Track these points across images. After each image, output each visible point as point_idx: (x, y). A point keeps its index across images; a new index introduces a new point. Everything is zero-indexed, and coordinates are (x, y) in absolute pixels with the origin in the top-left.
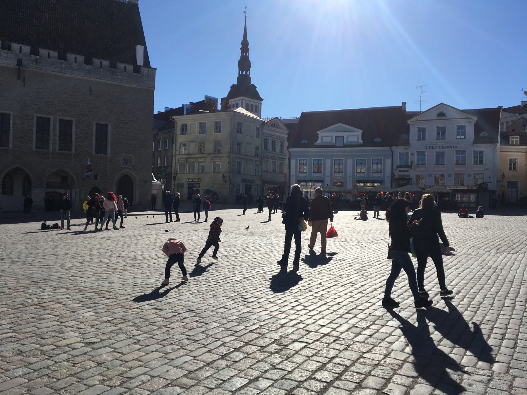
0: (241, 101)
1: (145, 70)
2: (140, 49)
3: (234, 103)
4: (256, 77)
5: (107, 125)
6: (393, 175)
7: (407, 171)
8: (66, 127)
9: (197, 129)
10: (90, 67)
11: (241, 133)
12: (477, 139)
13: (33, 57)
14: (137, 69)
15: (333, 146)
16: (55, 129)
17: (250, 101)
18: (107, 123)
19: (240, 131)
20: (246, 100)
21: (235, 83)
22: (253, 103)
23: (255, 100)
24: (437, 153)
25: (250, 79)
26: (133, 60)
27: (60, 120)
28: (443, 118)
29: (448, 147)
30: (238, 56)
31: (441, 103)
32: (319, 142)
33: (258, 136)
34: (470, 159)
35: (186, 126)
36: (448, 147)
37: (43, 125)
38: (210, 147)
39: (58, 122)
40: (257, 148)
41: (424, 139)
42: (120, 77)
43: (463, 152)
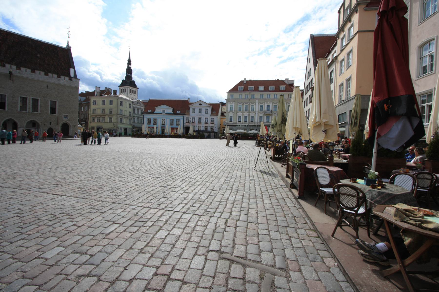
1: (74, 80)
2: (72, 70)
4: (135, 77)
5: (56, 102)
6: (184, 125)
8: (35, 102)
9: (101, 103)
10: (47, 77)
12: (212, 114)
13: (18, 71)
14: (70, 78)
16: (29, 102)
19: (121, 105)
21: (125, 79)
25: (132, 78)
26: (68, 75)
27: (32, 99)
30: (126, 66)
32: (156, 112)
33: (130, 107)
34: (209, 121)
35: (95, 101)
37: (24, 100)
38: (107, 112)
39: (31, 100)
40: (130, 112)
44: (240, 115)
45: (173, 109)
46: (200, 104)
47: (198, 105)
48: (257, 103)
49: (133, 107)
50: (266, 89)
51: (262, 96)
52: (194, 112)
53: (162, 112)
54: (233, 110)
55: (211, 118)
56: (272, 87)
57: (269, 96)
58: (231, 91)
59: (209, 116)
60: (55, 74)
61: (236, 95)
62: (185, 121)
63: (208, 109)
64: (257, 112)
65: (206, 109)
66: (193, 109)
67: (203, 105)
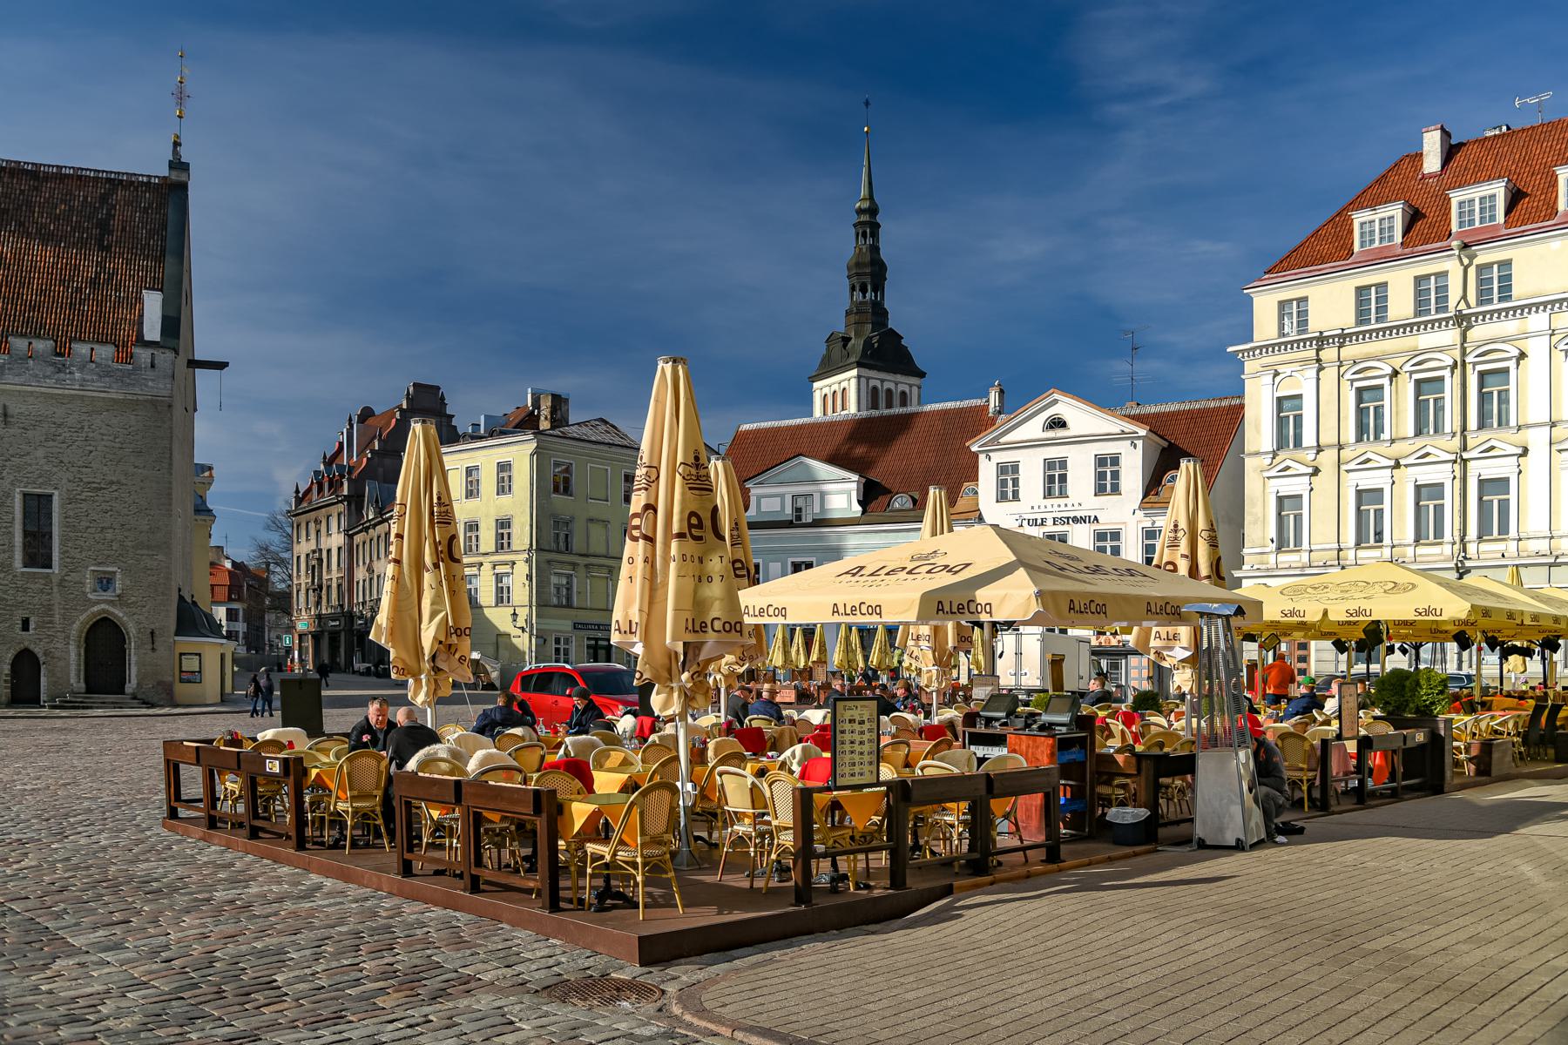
0: (854, 382)
3: (835, 387)
5: (51, 496)
11: (567, 491)
15: (789, 524)
17: (882, 381)
18: (48, 491)
20: (868, 379)
22: (892, 386)
23: (899, 378)
28: (1060, 433)
29: (1076, 520)
36: (1076, 520)
42: (77, 375)
43: (1116, 535)
52: (1008, 487)
60: (39, 337)
63: (1115, 460)
65: (1101, 461)
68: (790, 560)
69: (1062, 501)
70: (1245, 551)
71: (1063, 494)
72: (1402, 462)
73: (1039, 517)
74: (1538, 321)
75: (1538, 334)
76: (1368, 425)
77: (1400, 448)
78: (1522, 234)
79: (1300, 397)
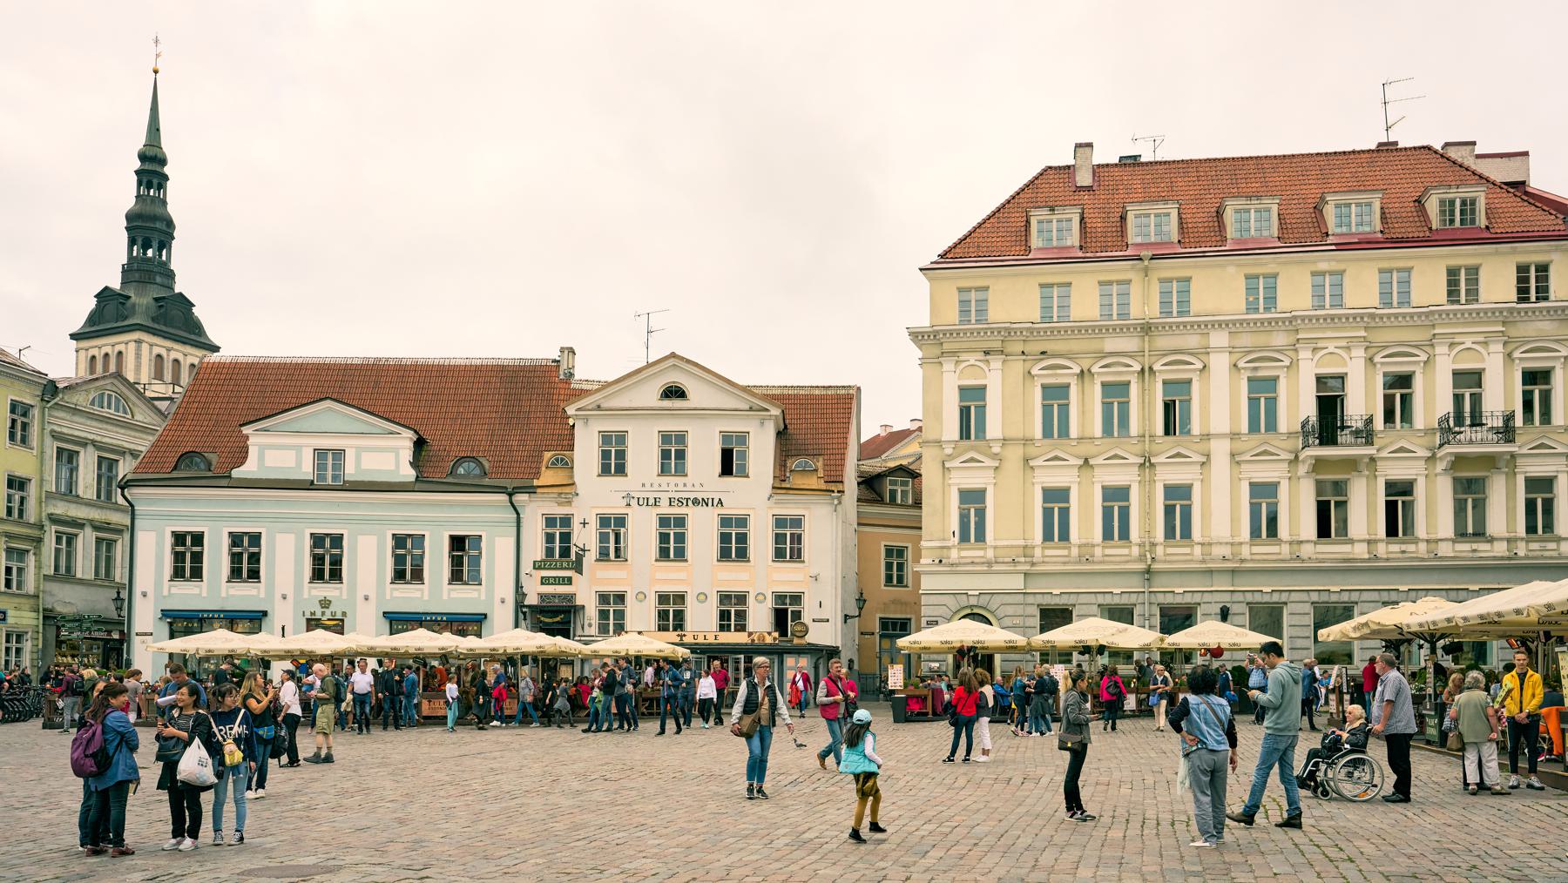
7: (569, 581)
15: (309, 486)
24: (664, 521)
29: (696, 502)
31: (673, 355)
34: (761, 540)
36: (696, 502)
41: (621, 470)
43: (742, 521)
44: (1057, 479)
45: (420, 444)
46: (673, 392)
47: (649, 395)
48: (1220, 363)
49: (56, 436)
50: (1304, 231)
51: (1263, 292)
52: (614, 462)
53: (307, 470)
54: (994, 429)
55: (780, 522)
56: (1355, 212)
57: (1329, 288)
58: (953, 256)
59: (753, 496)
61: (1014, 298)
62: (535, 548)
64: (1220, 450)
66: (606, 438)
67: (698, 395)
68: (910, 545)
69: (680, 480)
70: (924, 544)
71: (681, 471)
72: (1091, 462)
73: (651, 496)
74: (1219, 339)
75: (1220, 350)
76: (1055, 421)
77: (1086, 449)
78: (1203, 255)
79: (984, 388)
